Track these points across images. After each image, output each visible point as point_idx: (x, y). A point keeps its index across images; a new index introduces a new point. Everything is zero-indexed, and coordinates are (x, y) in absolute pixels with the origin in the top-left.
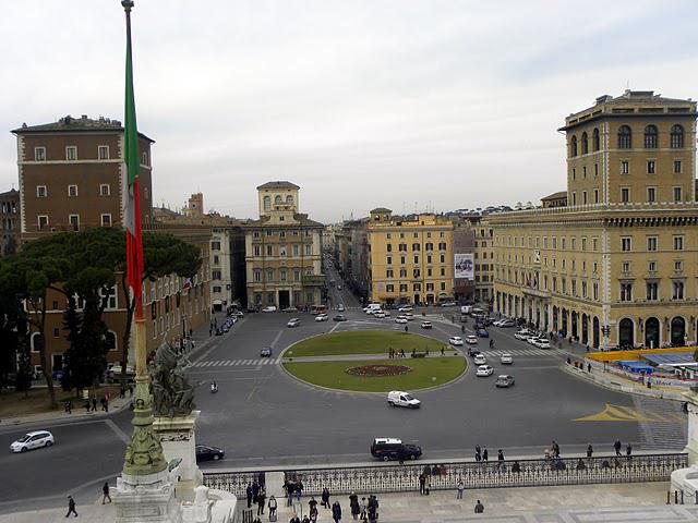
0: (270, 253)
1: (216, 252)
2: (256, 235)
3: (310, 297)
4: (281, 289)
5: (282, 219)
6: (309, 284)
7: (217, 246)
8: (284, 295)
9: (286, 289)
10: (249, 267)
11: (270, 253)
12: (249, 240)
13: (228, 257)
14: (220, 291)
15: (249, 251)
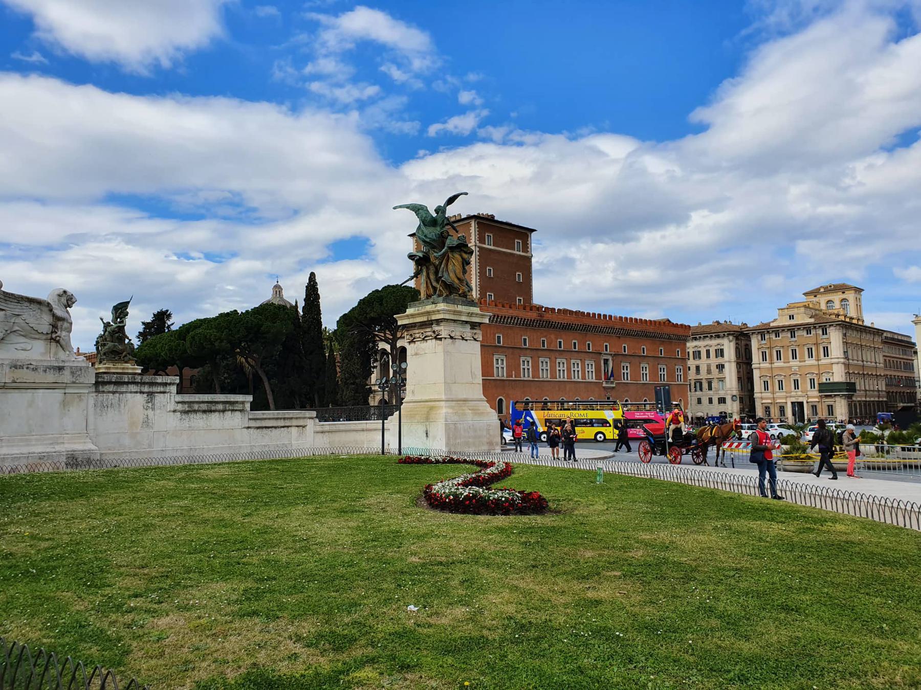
0: (779, 357)
1: (720, 360)
2: (763, 338)
3: (831, 409)
4: (794, 400)
5: (792, 317)
6: (827, 389)
7: (720, 353)
8: (798, 407)
9: (800, 400)
10: (756, 374)
11: (779, 357)
12: (755, 343)
13: (734, 365)
14: (725, 402)
15: (756, 357)
